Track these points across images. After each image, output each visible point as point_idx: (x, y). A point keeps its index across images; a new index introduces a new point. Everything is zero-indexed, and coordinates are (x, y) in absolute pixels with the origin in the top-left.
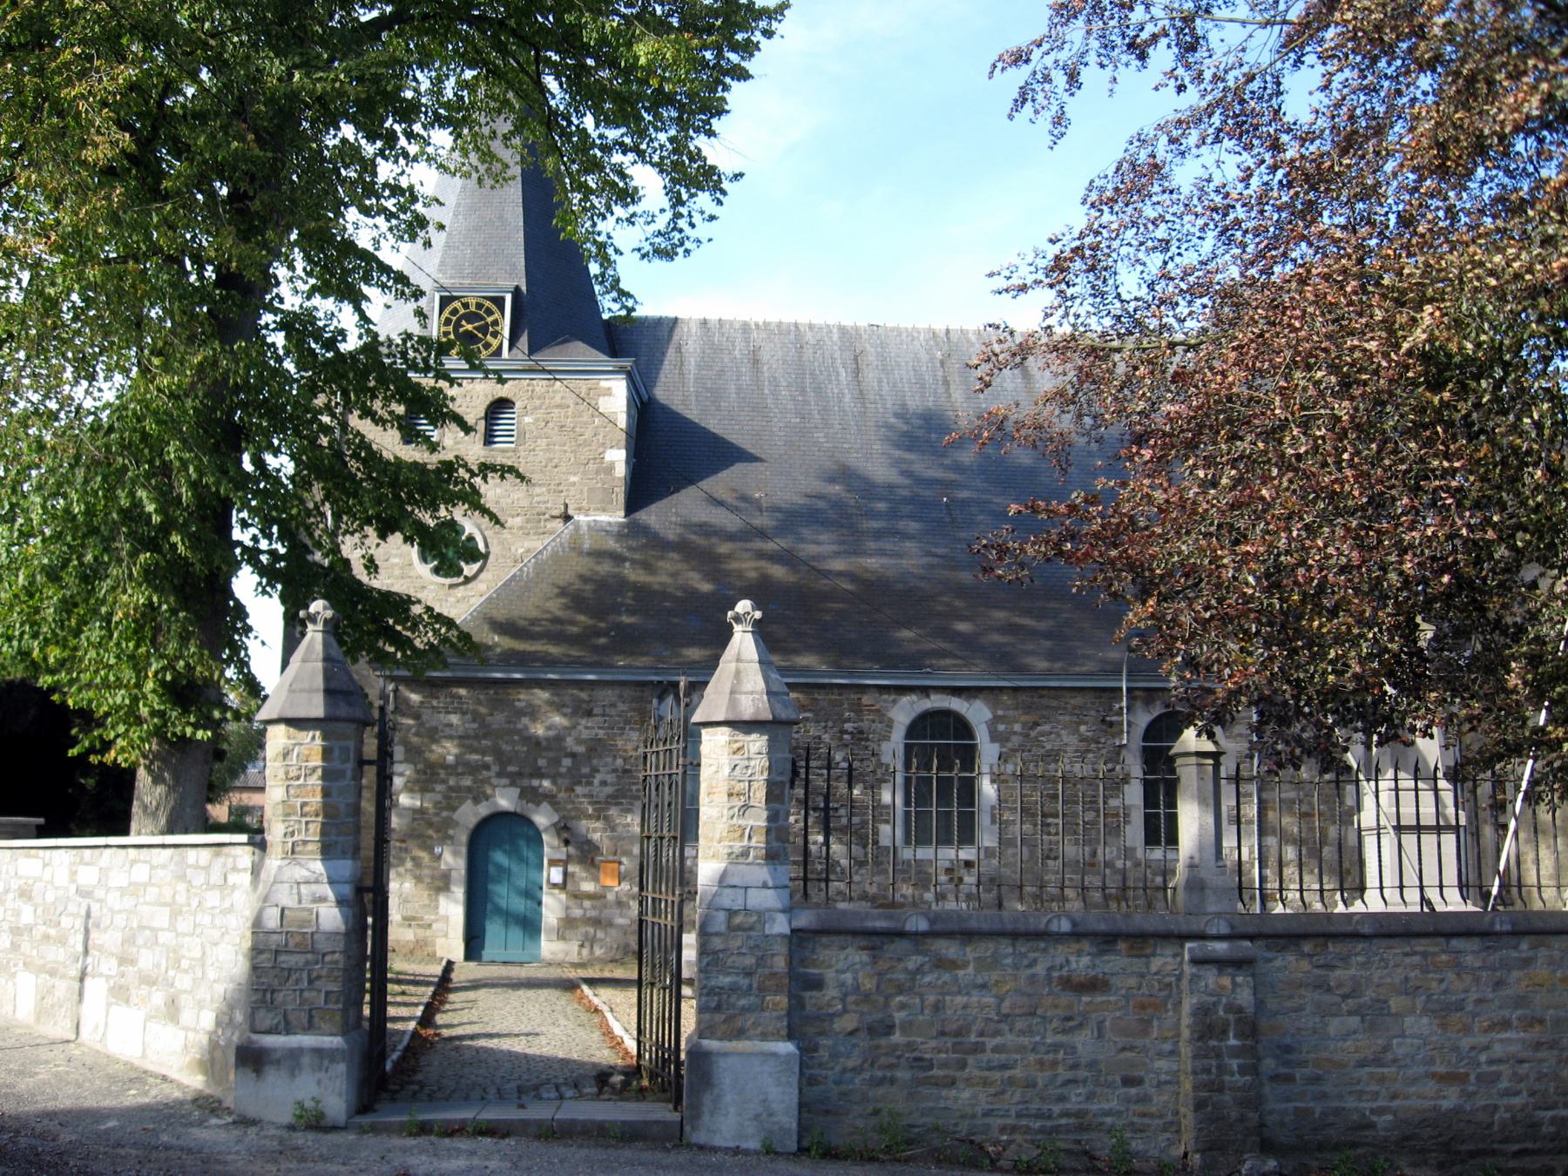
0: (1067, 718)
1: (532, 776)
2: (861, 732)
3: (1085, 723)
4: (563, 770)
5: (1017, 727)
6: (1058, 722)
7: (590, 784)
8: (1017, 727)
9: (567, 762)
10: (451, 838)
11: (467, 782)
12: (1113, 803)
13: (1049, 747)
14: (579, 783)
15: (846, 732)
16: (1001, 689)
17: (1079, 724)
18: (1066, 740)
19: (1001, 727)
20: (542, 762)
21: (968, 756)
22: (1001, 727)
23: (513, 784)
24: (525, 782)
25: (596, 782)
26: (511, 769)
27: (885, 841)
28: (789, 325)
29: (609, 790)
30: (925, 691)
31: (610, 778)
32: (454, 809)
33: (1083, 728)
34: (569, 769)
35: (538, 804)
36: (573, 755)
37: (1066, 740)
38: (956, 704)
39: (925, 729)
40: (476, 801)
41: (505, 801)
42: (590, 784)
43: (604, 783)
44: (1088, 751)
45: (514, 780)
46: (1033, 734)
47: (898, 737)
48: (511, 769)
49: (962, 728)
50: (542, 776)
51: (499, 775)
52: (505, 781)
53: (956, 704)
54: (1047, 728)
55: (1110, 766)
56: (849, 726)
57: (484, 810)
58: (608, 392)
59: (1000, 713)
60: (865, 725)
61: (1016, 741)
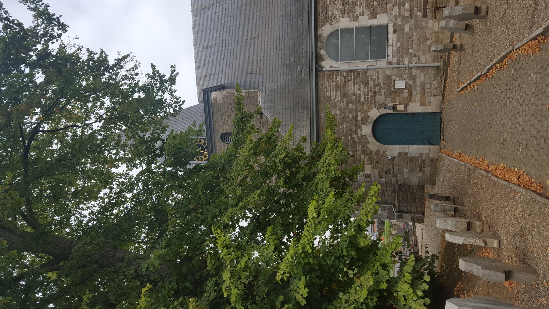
1: (357, 121)
4: (354, 107)
7: (360, 95)
9: (350, 105)
10: (384, 153)
11: (359, 147)
14: (359, 100)
20: (351, 116)
23: (360, 128)
24: (359, 122)
25: (359, 93)
26: (354, 128)
28: (194, 36)
29: (362, 86)
31: (357, 86)
32: (371, 152)
34: (353, 104)
35: (369, 117)
36: (347, 104)
40: (368, 143)
41: (367, 130)
42: (360, 95)
43: (359, 90)
45: (358, 127)
48: (354, 128)
50: (357, 116)
51: (356, 133)
52: (359, 131)
57: (372, 139)
58: (215, 99)
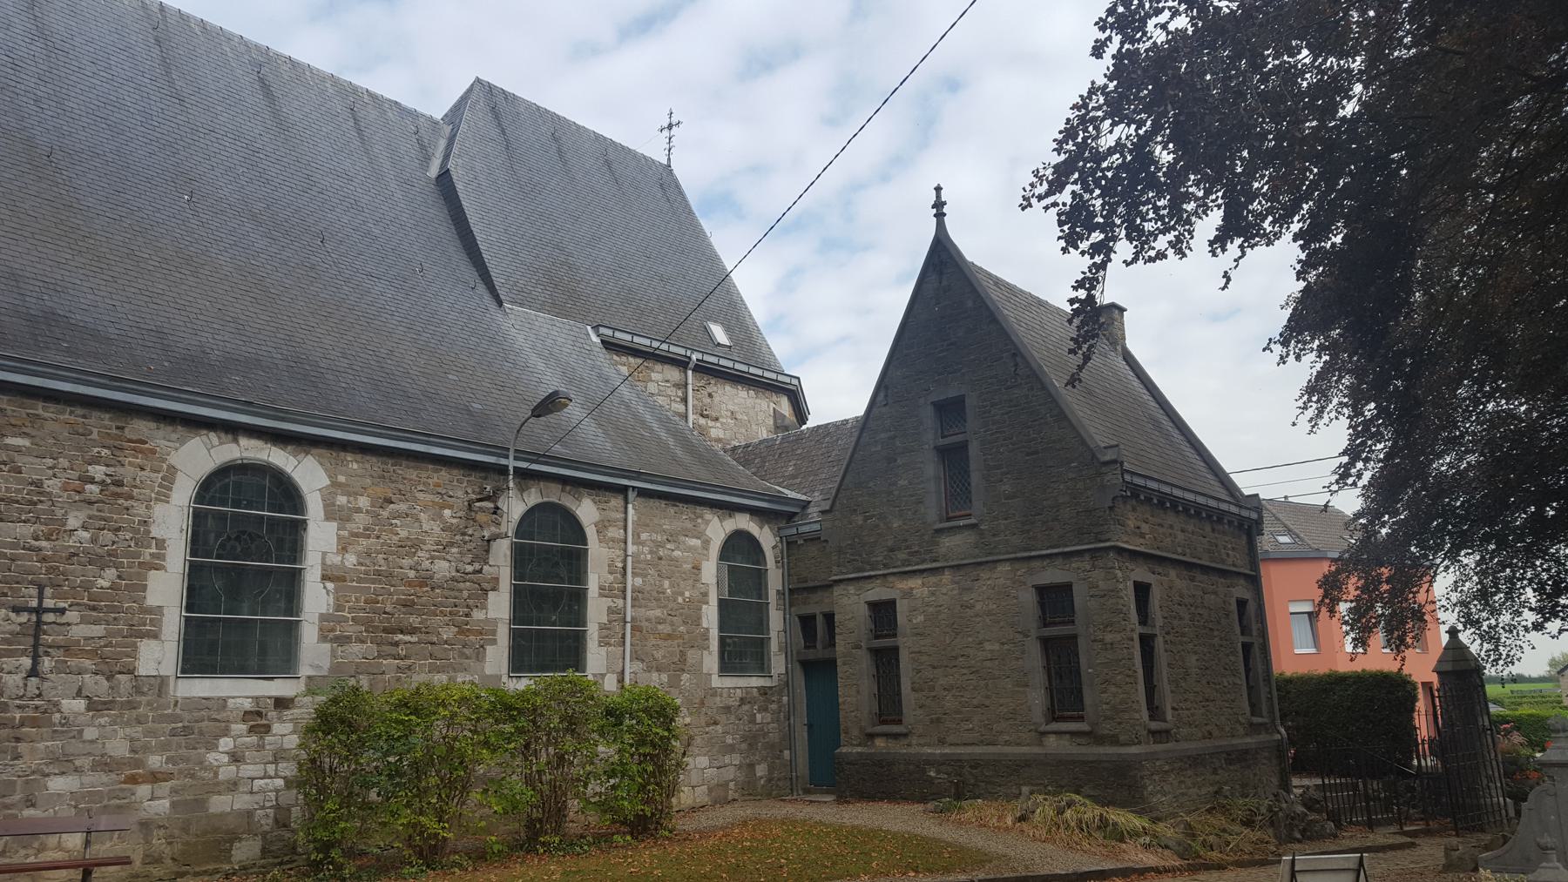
0: (429, 497)
2: (119, 484)
3: (451, 507)
5: (363, 502)
6: (416, 500)
8: (363, 502)
12: (478, 615)
13: (403, 534)
15: (92, 481)
16: (345, 446)
17: (443, 507)
18: (426, 527)
19: (342, 500)
21: (291, 537)
22: (342, 500)
27: (145, 667)
30: (232, 430)
33: (447, 512)
37: (426, 527)
38: (278, 457)
39: (225, 489)
44: (452, 544)
46: (385, 514)
47: (184, 493)
49: (287, 493)
53: (278, 457)
54: (403, 507)
55: (477, 566)
56: (98, 471)
59: (342, 479)
60: (127, 473)
61: (361, 521)
